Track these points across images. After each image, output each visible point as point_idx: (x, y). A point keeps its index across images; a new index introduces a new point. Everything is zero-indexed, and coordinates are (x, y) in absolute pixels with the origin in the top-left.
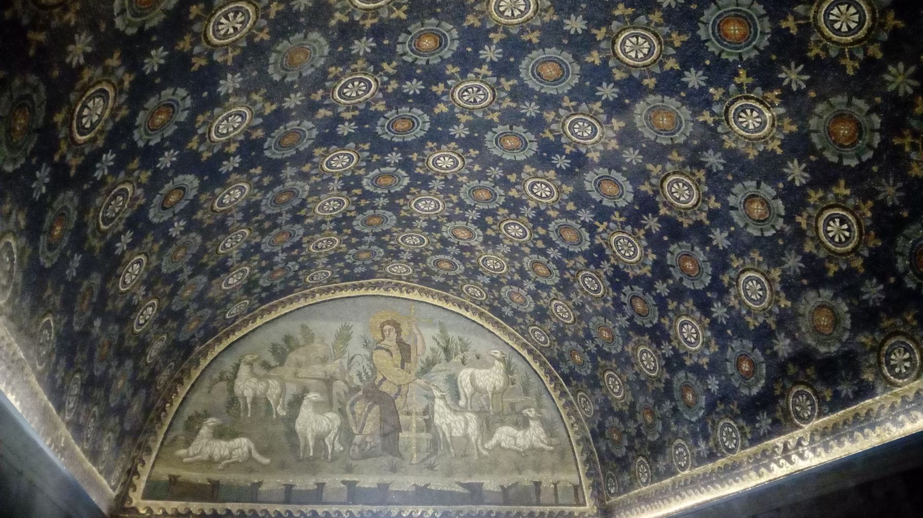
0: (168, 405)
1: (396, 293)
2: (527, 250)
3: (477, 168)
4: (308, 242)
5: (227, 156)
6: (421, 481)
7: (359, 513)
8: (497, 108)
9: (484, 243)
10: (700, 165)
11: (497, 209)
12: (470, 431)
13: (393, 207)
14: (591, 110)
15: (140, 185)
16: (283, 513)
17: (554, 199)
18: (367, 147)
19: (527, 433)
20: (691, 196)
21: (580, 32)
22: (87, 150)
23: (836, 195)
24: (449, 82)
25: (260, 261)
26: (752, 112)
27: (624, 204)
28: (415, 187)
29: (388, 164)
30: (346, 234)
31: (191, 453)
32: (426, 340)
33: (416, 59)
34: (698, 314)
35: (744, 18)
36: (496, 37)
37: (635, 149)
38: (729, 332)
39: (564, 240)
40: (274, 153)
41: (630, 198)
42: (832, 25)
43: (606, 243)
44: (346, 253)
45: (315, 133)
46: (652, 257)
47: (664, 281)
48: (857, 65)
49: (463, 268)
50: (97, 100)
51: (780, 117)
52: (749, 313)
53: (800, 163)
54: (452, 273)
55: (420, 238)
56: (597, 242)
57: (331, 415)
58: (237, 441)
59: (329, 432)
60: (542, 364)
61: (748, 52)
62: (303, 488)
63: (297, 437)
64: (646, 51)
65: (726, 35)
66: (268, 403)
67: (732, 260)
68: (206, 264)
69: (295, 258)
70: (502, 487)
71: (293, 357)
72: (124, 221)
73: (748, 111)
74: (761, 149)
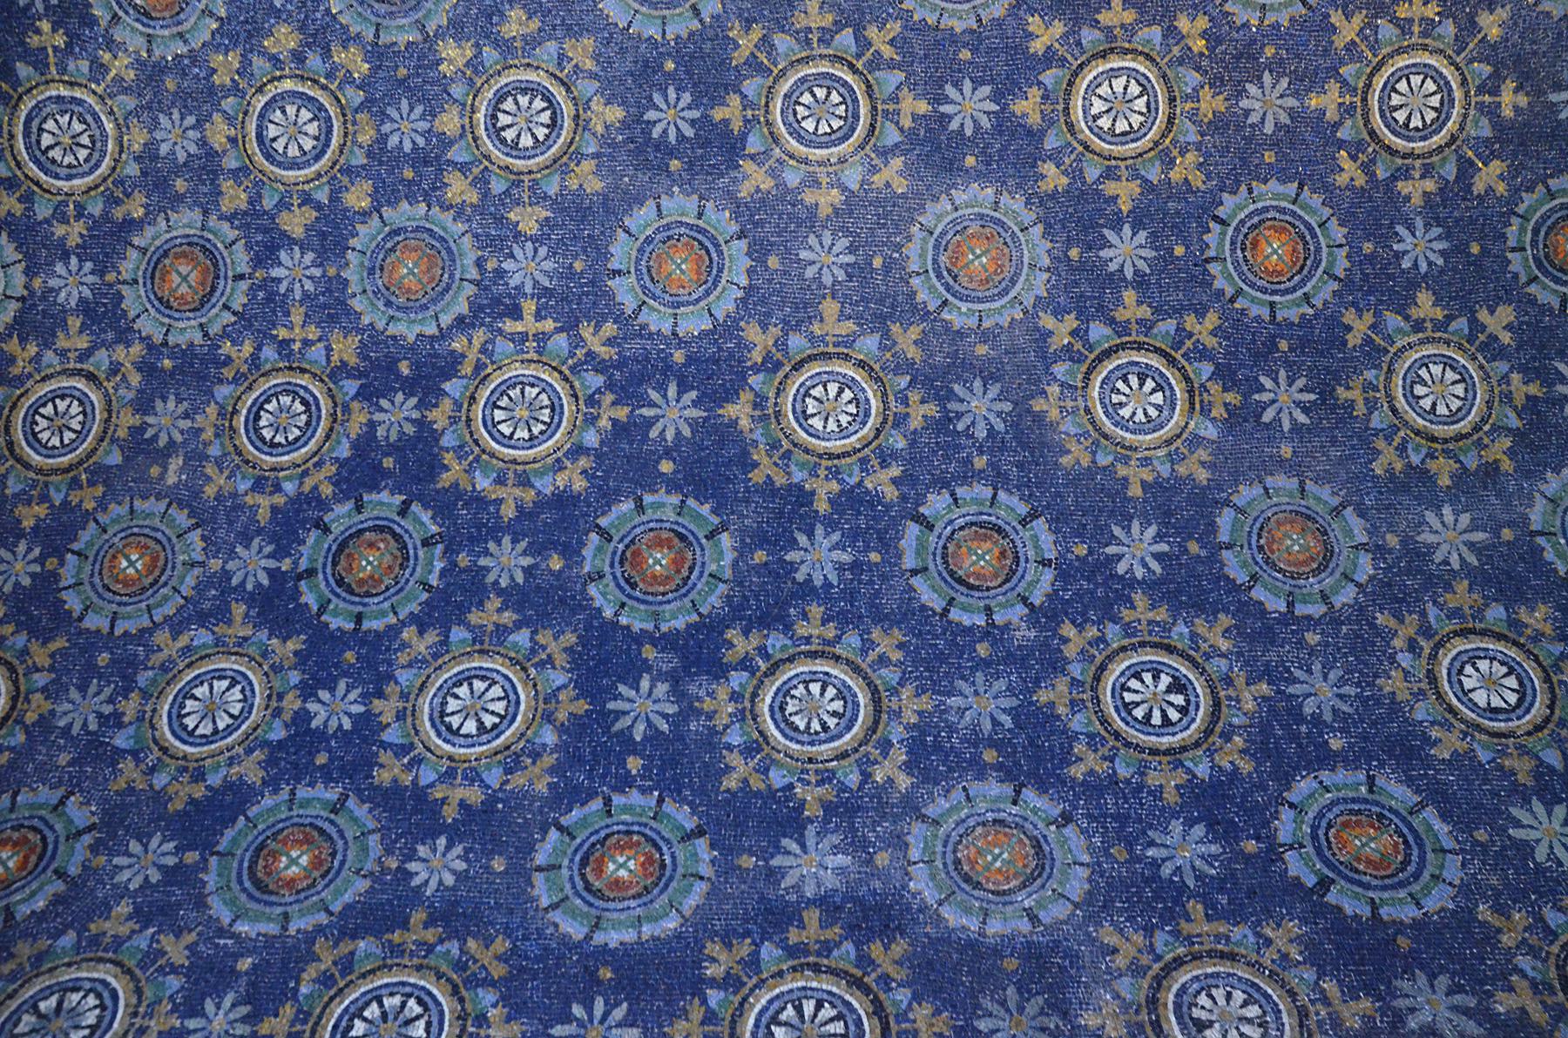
2: (234, 197)
9: (151, 72)
14: (895, 99)
20: (843, 432)
23: (1194, 636)
26: (1154, 391)
37: (852, 249)
41: (694, 323)
42: (1414, 382)
43: (479, 366)
46: (573, 479)
48: (1399, 466)
51: (1196, 441)
53: (1159, 538)
61: (1253, 300)
64: (1121, 126)
65: (1255, 244)
74: (1104, 460)
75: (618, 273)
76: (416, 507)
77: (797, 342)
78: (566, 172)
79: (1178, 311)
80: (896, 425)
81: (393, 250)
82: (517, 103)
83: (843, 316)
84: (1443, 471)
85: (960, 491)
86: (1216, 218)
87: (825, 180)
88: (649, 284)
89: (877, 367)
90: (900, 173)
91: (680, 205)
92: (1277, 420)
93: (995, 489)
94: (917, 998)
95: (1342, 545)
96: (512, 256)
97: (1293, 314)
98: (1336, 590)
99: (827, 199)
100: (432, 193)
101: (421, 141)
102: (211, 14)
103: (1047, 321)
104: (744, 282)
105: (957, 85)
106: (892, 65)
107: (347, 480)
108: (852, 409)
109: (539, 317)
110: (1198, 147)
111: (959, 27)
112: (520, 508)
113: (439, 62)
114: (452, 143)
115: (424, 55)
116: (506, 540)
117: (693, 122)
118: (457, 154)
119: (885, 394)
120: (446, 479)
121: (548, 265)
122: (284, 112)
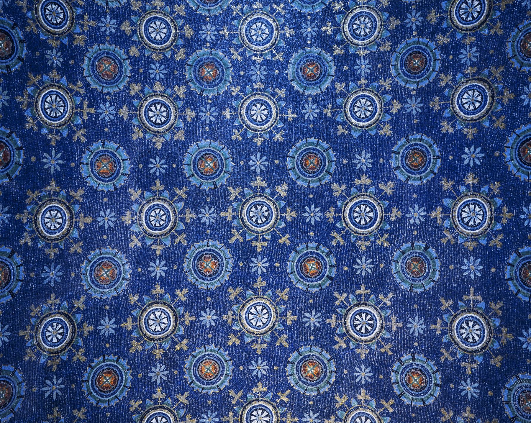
5: (475, 169)
11: (188, 54)
18: (341, 130)
20: (44, 224)
21: (203, 313)
24: (283, 225)
33: (317, 248)
35: (108, 392)
36: (260, 283)
37: (110, 228)
40: (431, 146)
41: (85, 170)
43: (71, 90)
51: (39, 355)
61: (90, 374)
64: (151, 322)
65: (110, 373)
74: (32, 321)
75: (103, 144)
76: (21, 63)
77: (77, 207)
78: (140, 127)
79: (86, 346)
80: (46, 244)
81: (115, 62)
82: (164, 111)
83: (86, 224)
85: (22, 268)
86: (119, 358)
87: (134, 219)
88: (99, 155)
89: (67, 237)
90: (136, 245)
91: (127, 167)
92: (46, 385)
93: (22, 281)
96: (111, 106)
97: (84, 389)
99: (127, 219)
100: (134, 79)
101: (152, 76)
102: (198, 8)
103: (83, 299)
104: (99, 189)
105: (165, 265)
106: (172, 242)
107: (31, 37)
108: (53, 228)
109: (89, 114)
110: (144, 350)
111: (185, 265)
112: (20, 103)
113: (179, 86)
114: (151, 87)
115: (181, 81)
116: (8, 98)
117: (155, 173)
118: (147, 88)
119: (57, 240)
120: (31, 76)
121: (107, 118)
122: (164, 28)
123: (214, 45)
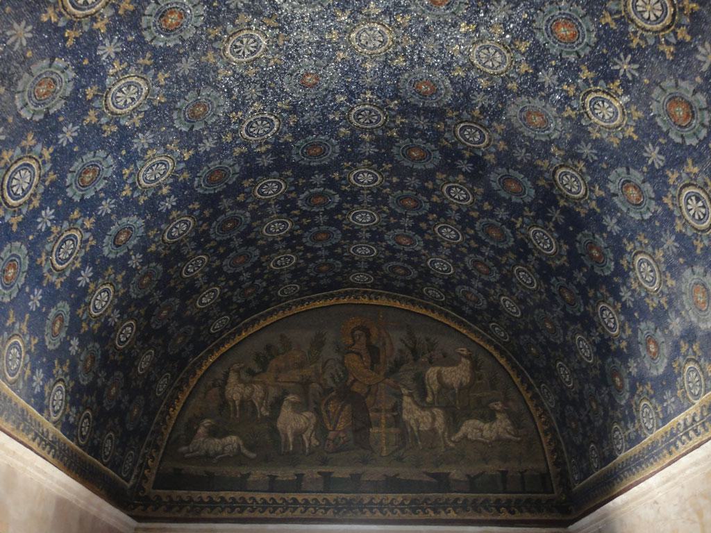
0: (171, 409)
1: (366, 301)
3: (395, 180)
4: (267, 261)
5: (164, 198)
6: (391, 471)
7: (335, 500)
8: (392, 125)
9: (425, 247)
10: (578, 157)
12: (437, 425)
13: (332, 222)
14: (473, 117)
15: (87, 230)
16: (268, 500)
17: (471, 200)
18: (289, 173)
19: (494, 425)
22: (24, 211)
23: (688, 174)
25: (227, 281)
27: (530, 200)
28: (348, 202)
29: (315, 186)
30: (300, 251)
31: (191, 450)
32: (396, 341)
34: (611, 299)
38: (636, 314)
39: (492, 239)
40: (206, 190)
43: (527, 238)
44: (307, 268)
45: (237, 168)
46: (565, 247)
47: (580, 271)
49: (416, 272)
50: (23, 172)
51: (627, 105)
52: (647, 295)
54: (409, 278)
55: (369, 248)
56: (519, 237)
57: (307, 414)
58: (228, 438)
59: (307, 428)
60: (509, 360)
62: (285, 479)
63: (278, 434)
64: (499, 59)
66: (254, 405)
67: (625, 245)
68: (174, 288)
69: (260, 276)
70: (468, 476)
71: (273, 363)
72: (80, 260)
73: (600, 103)
74: (621, 136)
77: (547, 175)
84: (682, 34)
91: (493, 176)
92: (633, 76)
94: (705, 361)
95: (689, 96)
98: (703, 118)
104: (522, 176)
108: (573, 179)
115: (434, 204)
123: (402, 216)
